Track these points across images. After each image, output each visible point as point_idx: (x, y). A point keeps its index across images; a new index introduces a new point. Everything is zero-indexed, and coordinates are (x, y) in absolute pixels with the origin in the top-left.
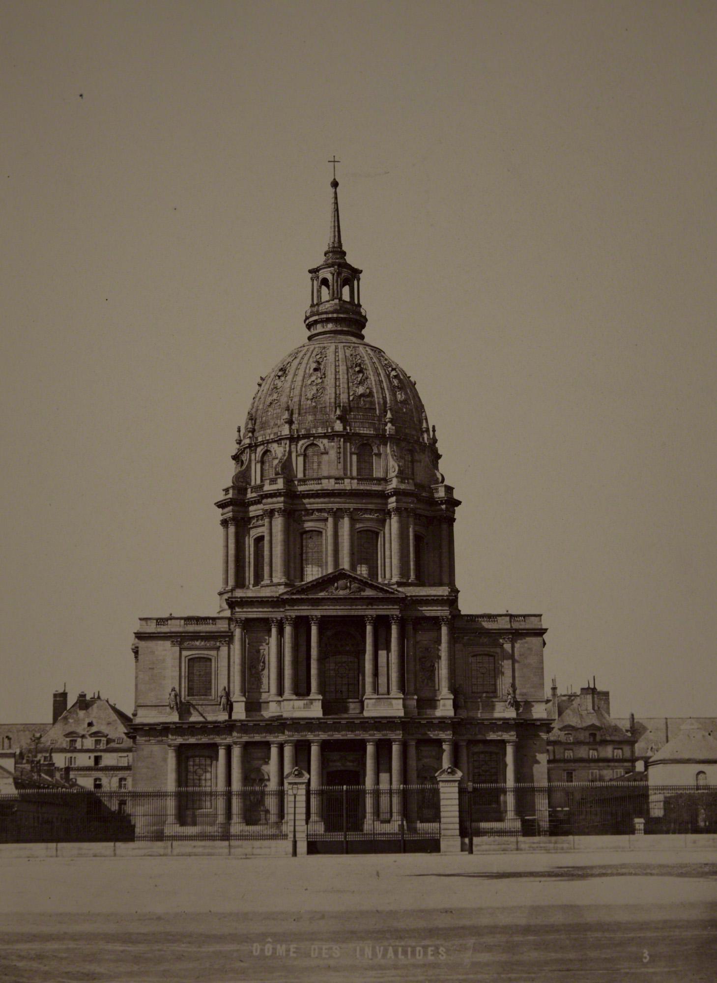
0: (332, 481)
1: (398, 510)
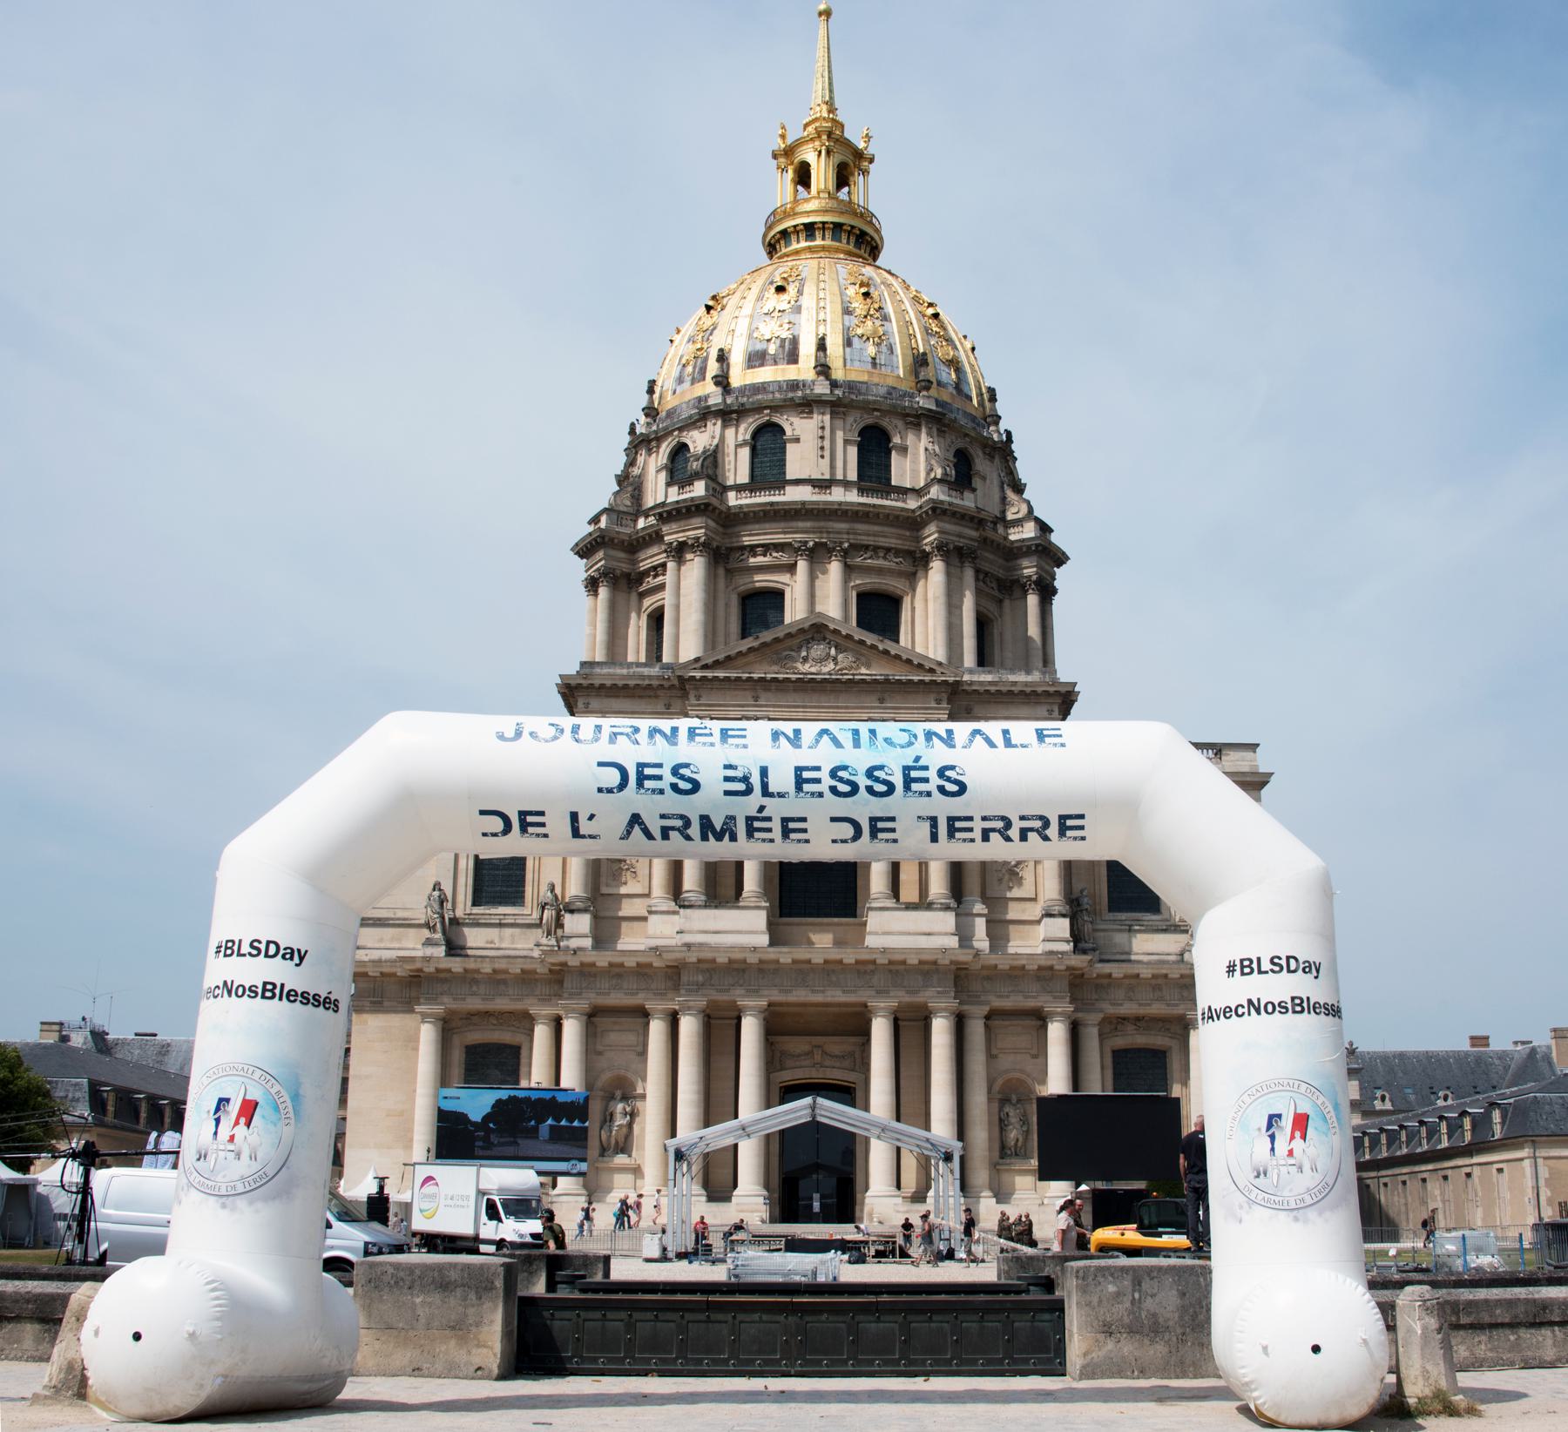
0: (809, 488)
1: (943, 549)
